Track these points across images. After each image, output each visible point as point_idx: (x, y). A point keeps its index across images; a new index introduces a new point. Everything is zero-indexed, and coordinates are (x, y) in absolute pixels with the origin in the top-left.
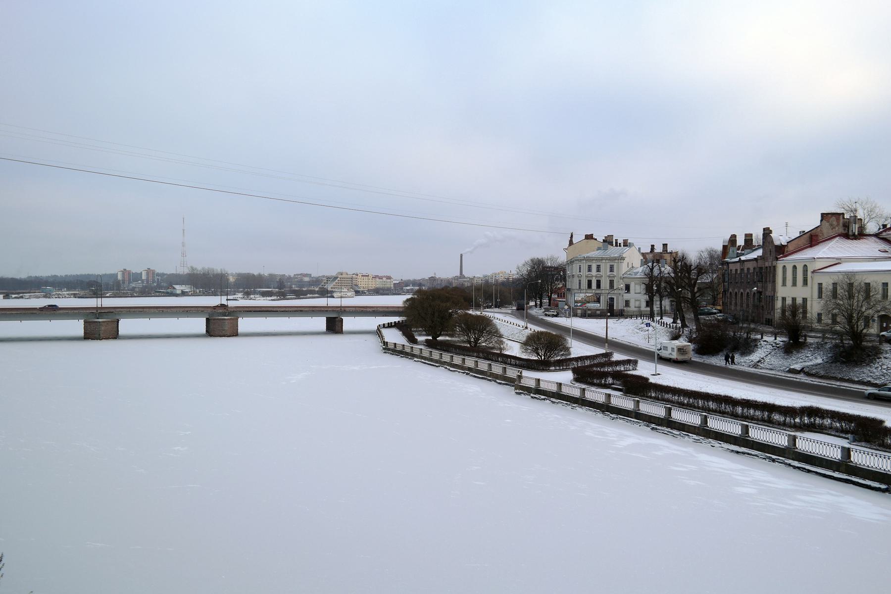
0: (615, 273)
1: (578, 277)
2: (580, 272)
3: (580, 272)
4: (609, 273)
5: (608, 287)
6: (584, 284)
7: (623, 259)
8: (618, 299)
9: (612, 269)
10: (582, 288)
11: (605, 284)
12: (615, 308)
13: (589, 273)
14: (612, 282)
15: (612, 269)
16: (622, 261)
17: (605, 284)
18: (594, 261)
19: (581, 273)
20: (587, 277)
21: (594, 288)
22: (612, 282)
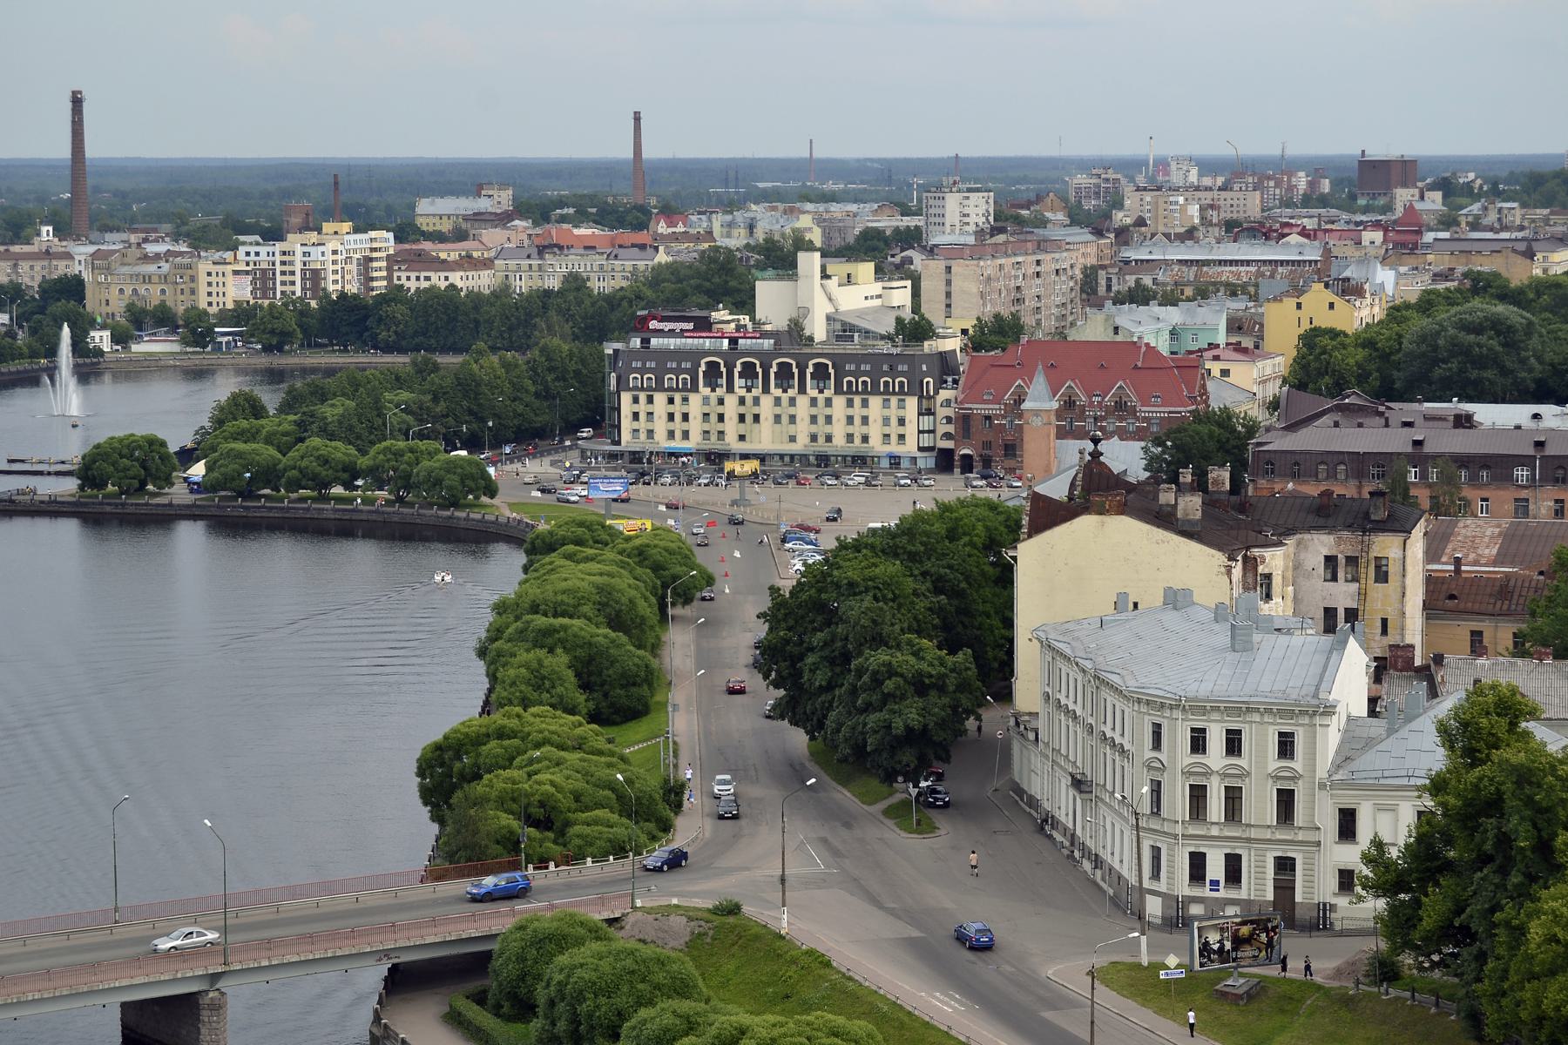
0: (1298, 764)
1: (1150, 768)
2: (1157, 744)
3: (1157, 744)
4: (1273, 763)
5: (1271, 813)
6: (1177, 801)
7: (1329, 710)
8: (1309, 870)
9: (1286, 746)
10: (1164, 813)
11: (1260, 806)
12: (1298, 898)
13: (1198, 758)
14: (1286, 800)
15: (1286, 746)
16: (1326, 721)
17: (1260, 806)
18: (1215, 716)
19: (1163, 756)
20: (1187, 774)
21: (1214, 819)
22: (1286, 800)
